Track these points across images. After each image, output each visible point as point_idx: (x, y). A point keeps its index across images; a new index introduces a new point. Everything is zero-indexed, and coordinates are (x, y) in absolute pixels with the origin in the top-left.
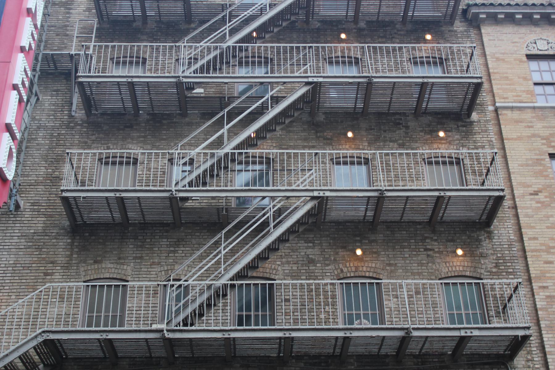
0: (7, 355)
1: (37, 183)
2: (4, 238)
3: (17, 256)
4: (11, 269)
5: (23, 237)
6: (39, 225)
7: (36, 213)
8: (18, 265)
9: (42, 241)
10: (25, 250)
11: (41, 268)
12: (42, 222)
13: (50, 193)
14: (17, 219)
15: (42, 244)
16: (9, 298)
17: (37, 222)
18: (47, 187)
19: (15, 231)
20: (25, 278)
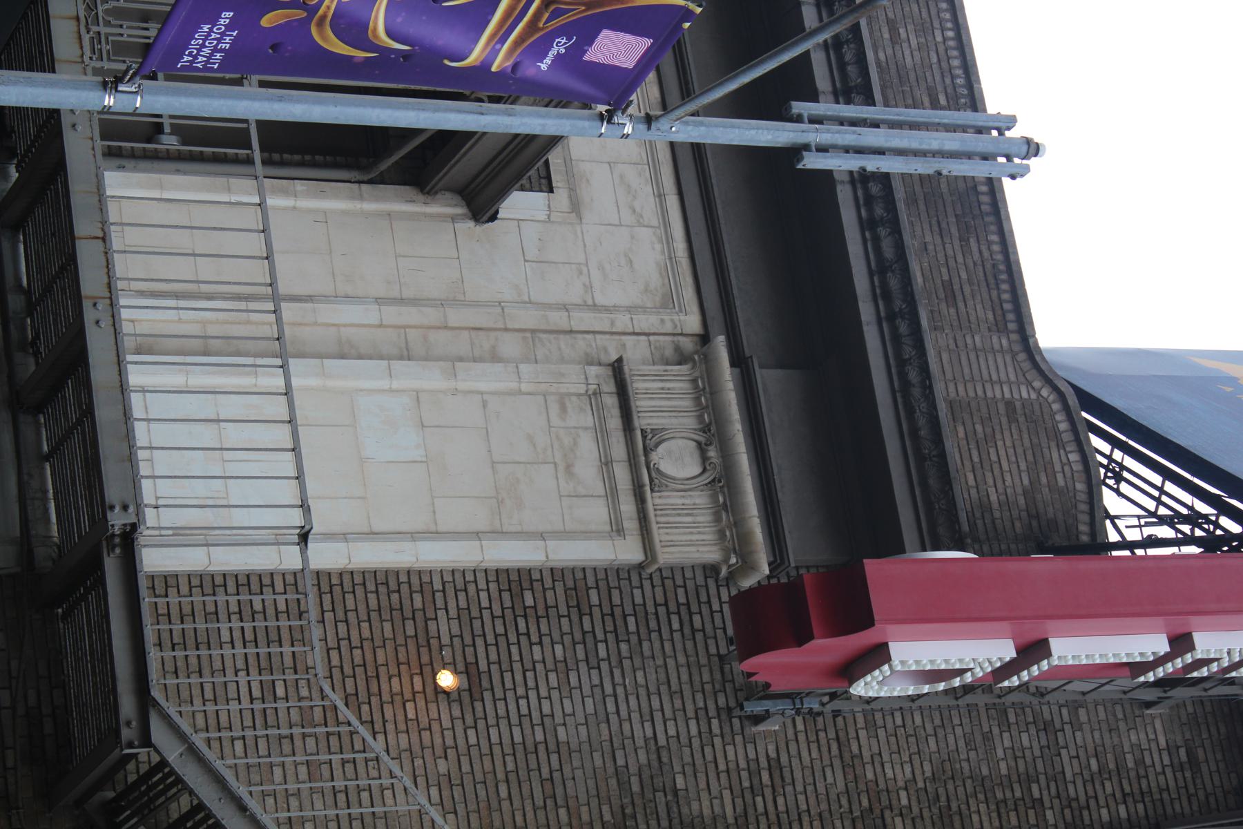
0: (243, 808)
1: (850, 764)
2: (642, 692)
3: (586, 747)
4: (539, 737)
5: (654, 757)
6: (706, 803)
7: (746, 784)
8: (554, 757)
10: (611, 770)
12: (717, 810)
13: (826, 815)
14: (715, 722)
16: (439, 751)
17: (715, 792)
18: (844, 801)
19: (671, 724)
20: (515, 792)
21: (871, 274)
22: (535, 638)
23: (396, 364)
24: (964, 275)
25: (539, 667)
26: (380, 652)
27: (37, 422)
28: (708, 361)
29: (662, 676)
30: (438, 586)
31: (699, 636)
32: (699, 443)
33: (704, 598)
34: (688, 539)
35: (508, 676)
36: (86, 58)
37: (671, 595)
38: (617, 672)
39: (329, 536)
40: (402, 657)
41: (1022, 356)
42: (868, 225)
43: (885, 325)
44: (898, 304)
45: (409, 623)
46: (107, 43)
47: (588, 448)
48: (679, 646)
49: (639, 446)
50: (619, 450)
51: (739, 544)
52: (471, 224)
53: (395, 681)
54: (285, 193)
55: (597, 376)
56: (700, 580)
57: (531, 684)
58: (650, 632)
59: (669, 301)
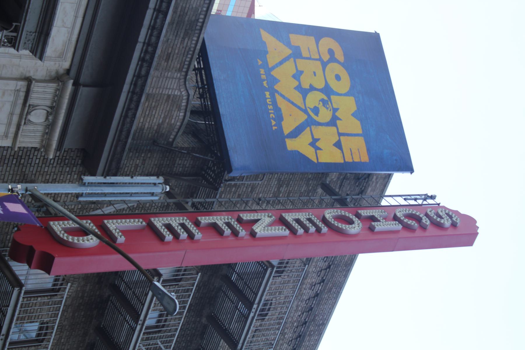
21: (134, 76)
24: (177, 51)
28: (64, 84)
32: (48, 112)
33: (28, 154)
34: (30, 138)
41: (182, 80)
42: (142, 60)
43: (130, 94)
44: (138, 90)
48: (12, 168)
49: (26, 106)
50: (18, 110)
55: (21, 85)
58: (4, 163)
59: (61, 56)
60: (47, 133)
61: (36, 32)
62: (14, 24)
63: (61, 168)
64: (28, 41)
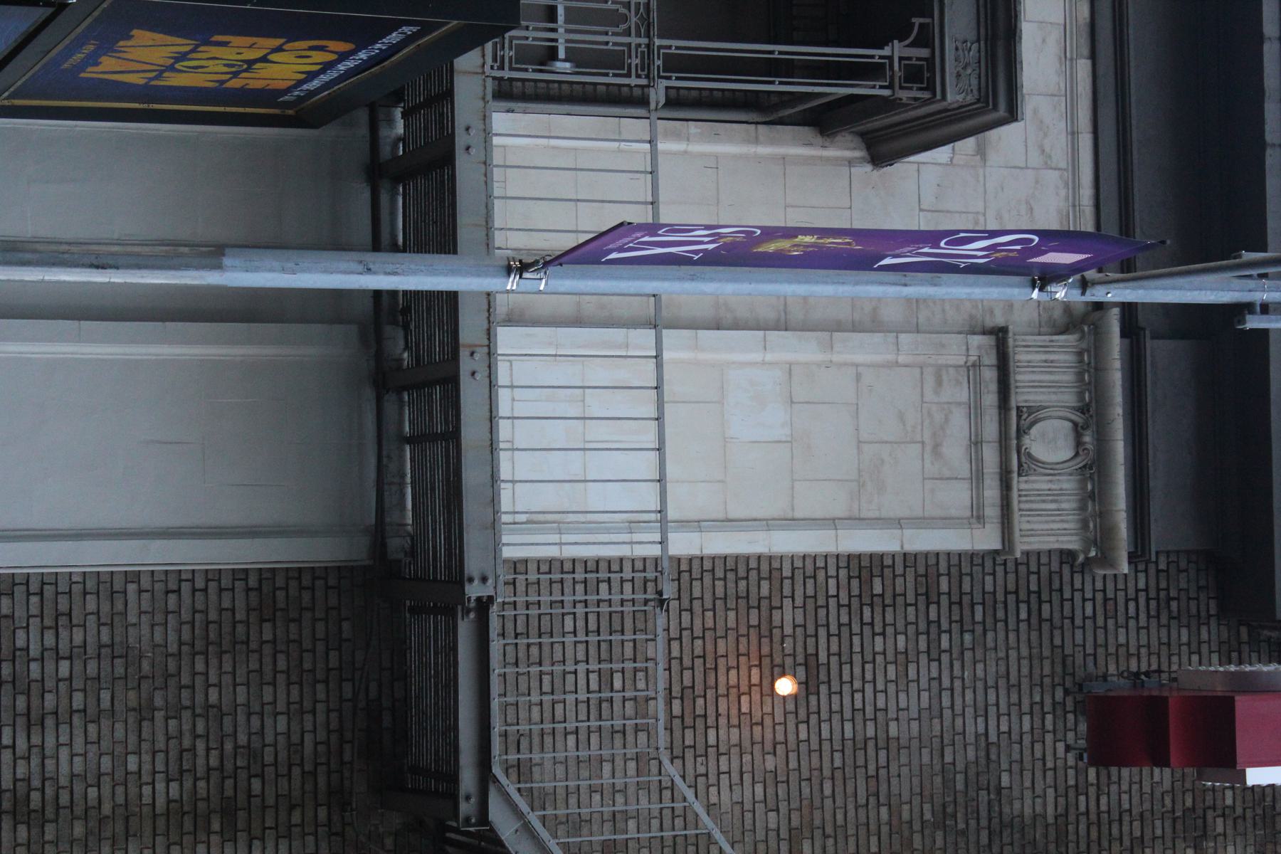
2: (980, 685)
3: (915, 743)
6: (1028, 802)
7: (1071, 782)
8: (882, 754)
9: (973, 823)
10: (938, 768)
11: (874, 840)
12: (1039, 809)
13: (1147, 815)
14: (1049, 718)
15: (961, 826)
16: (768, 747)
17: (1039, 790)
18: (1168, 801)
19: (1004, 719)
20: (839, 789)
22: (878, 629)
23: (773, 335)
25: (879, 659)
26: (721, 643)
27: (401, 401)
29: (1002, 669)
30: (787, 572)
31: (1046, 626)
32: (1075, 424)
33: (1056, 585)
34: (1049, 525)
35: (846, 668)
36: (487, 68)
37: (1022, 582)
38: (957, 665)
39: (684, 524)
40: (743, 649)
45: (754, 613)
46: (511, 49)
47: (959, 425)
48: (1023, 637)
49: (1013, 420)
50: (991, 429)
51: (1101, 538)
52: (869, 168)
53: (733, 673)
54: (677, 136)
55: (979, 347)
56: (1055, 566)
57: (869, 676)
58: (996, 621)
60: (1092, 496)
61: (978, 41)
62: (917, 21)
63: (1164, 632)
64: (965, 68)
